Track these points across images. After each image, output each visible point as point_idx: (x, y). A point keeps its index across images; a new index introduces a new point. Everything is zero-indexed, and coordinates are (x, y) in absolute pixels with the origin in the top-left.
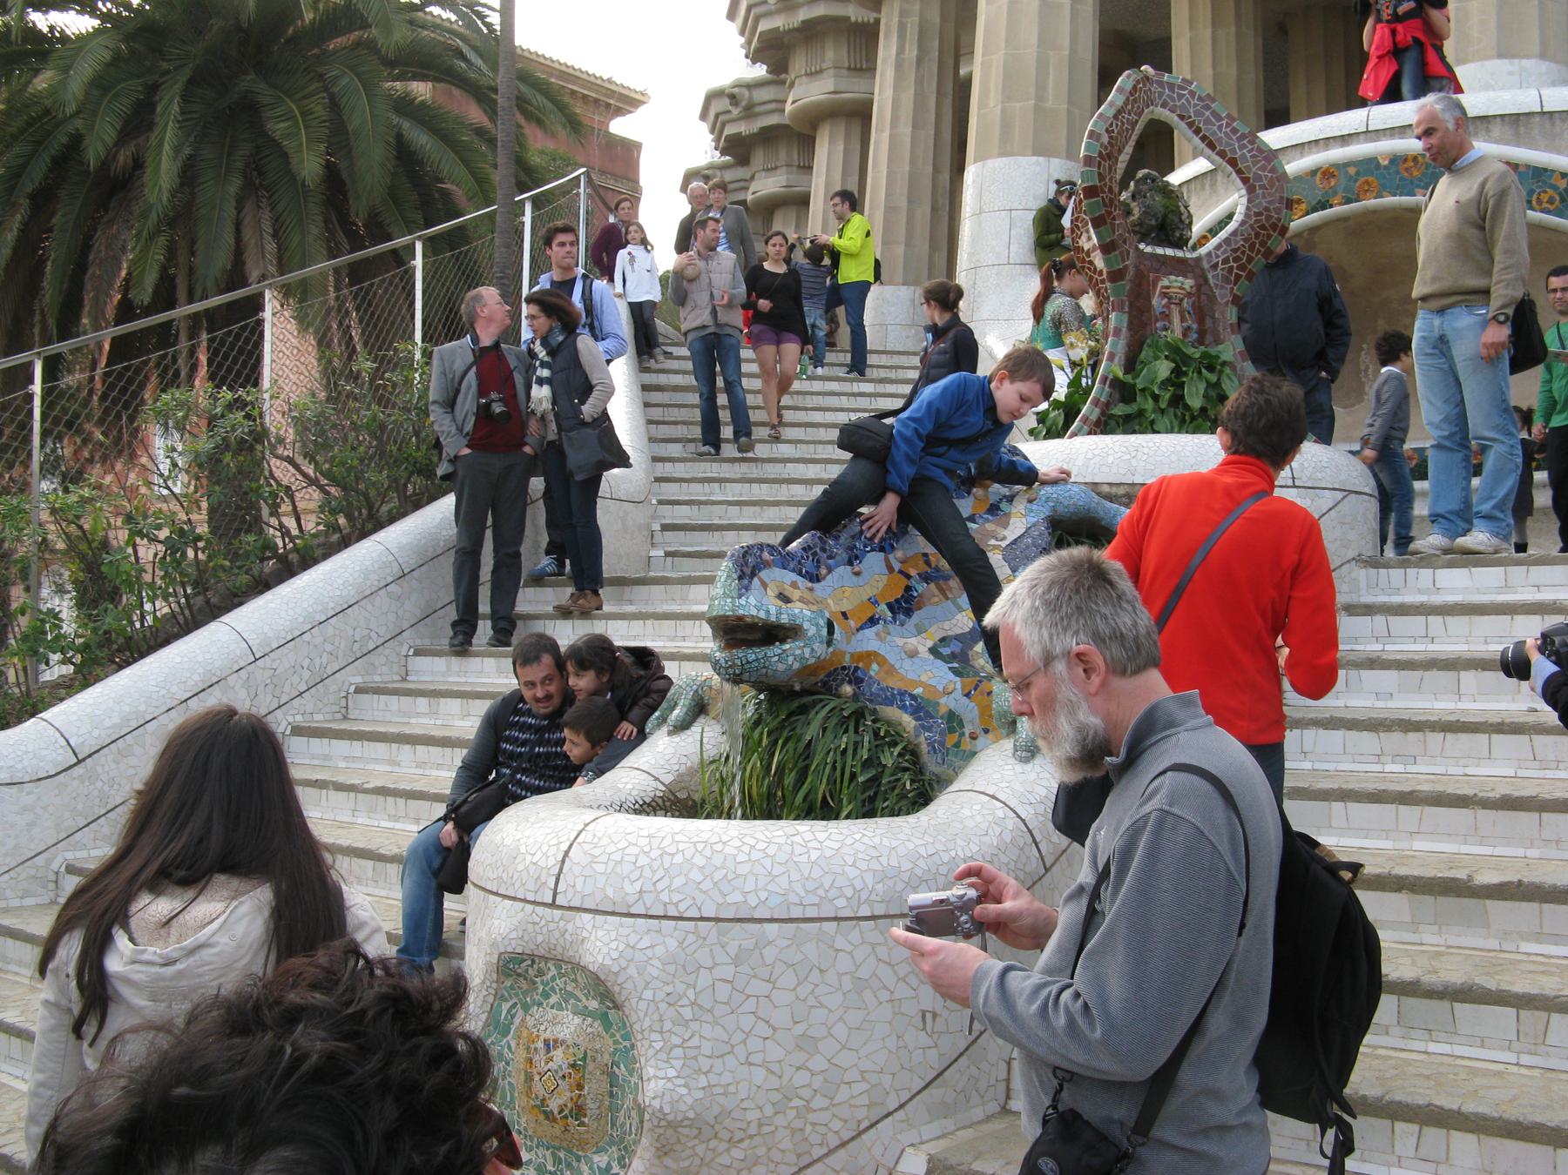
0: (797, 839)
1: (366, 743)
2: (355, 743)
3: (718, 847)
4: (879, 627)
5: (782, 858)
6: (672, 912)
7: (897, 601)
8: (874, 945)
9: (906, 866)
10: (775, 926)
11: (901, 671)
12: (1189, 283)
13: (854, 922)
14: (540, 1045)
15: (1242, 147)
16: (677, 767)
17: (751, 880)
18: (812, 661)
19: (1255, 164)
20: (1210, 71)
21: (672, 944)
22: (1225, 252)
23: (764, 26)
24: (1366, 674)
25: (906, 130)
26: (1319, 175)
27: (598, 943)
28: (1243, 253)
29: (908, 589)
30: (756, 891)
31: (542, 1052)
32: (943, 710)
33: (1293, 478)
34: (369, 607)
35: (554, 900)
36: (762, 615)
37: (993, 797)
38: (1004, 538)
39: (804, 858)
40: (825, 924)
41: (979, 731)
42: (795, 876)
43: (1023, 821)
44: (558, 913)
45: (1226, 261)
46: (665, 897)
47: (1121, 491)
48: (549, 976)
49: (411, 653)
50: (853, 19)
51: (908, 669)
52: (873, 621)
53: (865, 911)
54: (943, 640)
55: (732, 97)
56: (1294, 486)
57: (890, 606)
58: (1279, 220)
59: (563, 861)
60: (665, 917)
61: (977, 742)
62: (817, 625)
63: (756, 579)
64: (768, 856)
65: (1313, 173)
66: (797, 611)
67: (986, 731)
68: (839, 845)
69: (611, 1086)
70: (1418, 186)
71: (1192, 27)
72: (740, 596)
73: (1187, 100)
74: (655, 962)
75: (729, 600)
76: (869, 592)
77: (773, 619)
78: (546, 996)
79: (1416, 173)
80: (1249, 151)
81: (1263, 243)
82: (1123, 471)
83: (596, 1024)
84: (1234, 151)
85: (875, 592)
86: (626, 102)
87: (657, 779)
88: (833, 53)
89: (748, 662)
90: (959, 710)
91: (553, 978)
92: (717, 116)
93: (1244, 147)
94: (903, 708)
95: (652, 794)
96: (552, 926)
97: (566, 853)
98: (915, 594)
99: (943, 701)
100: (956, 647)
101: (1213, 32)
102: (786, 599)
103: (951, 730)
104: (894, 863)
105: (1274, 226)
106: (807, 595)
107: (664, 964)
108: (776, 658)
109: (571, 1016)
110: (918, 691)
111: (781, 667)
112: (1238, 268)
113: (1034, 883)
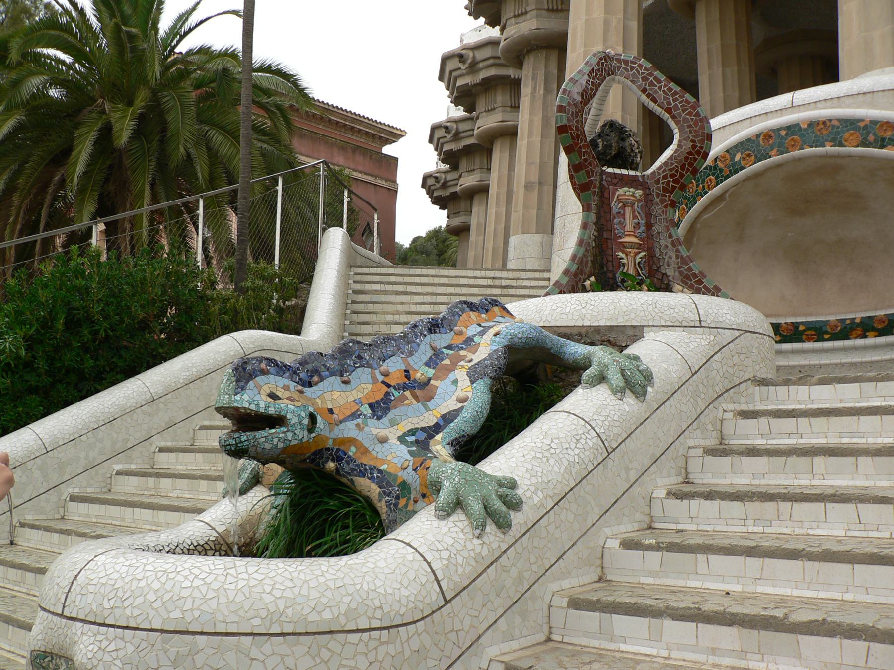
0: (233, 571)
1: (108, 506)
2: (102, 506)
3: (171, 576)
4: (359, 421)
5: (215, 585)
6: (132, 625)
7: (377, 402)
8: (282, 656)
9: (314, 594)
10: (204, 638)
11: (374, 453)
12: (639, 193)
13: (267, 637)
15: (675, 100)
16: (229, 521)
17: (190, 601)
18: (294, 442)
19: (684, 111)
20: (721, 95)
21: (130, 648)
23: (460, 83)
24: (746, 460)
25: (537, 139)
26: (762, 137)
28: (677, 171)
29: (387, 394)
30: (192, 610)
32: (399, 481)
33: (700, 321)
34: (129, 420)
35: (63, 612)
36: (253, 407)
37: (409, 545)
38: (470, 361)
39: (232, 586)
40: (243, 638)
41: (419, 496)
42: (223, 600)
43: (429, 564)
44: (64, 621)
45: (665, 177)
46: (128, 612)
47: (575, 331)
49: (157, 450)
50: (512, 77)
51: (378, 450)
52: (355, 415)
53: (276, 629)
54: (411, 430)
55: (446, 128)
56: (701, 327)
57: (371, 406)
58: (701, 148)
60: (127, 628)
62: (299, 416)
63: (251, 382)
64: (205, 583)
65: (758, 136)
66: (282, 406)
67: (424, 496)
68: (263, 577)
70: (827, 141)
71: (710, 68)
72: (236, 394)
73: (637, 70)
74: (118, 662)
75: (227, 396)
76: (355, 395)
77: (262, 410)
79: (825, 132)
80: (680, 103)
81: (691, 164)
82: (576, 317)
84: (669, 103)
85: (360, 395)
86: (393, 135)
87: (213, 528)
88: (501, 97)
89: (241, 442)
90: (409, 480)
92: (438, 139)
93: (676, 100)
94: (372, 479)
95: (206, 540)
98: (393, 398)
99: (400, 474)
100: (422, 436)
101: (723, 71)
102: (273, 396)
104: (304, 592)
105: (698, 153)
106: (296, 396)
107: (123, 664)
108: (263, 440)
110: (384, 467)
111: (268, 446)
112: (673, 182)
113: (433, 612)
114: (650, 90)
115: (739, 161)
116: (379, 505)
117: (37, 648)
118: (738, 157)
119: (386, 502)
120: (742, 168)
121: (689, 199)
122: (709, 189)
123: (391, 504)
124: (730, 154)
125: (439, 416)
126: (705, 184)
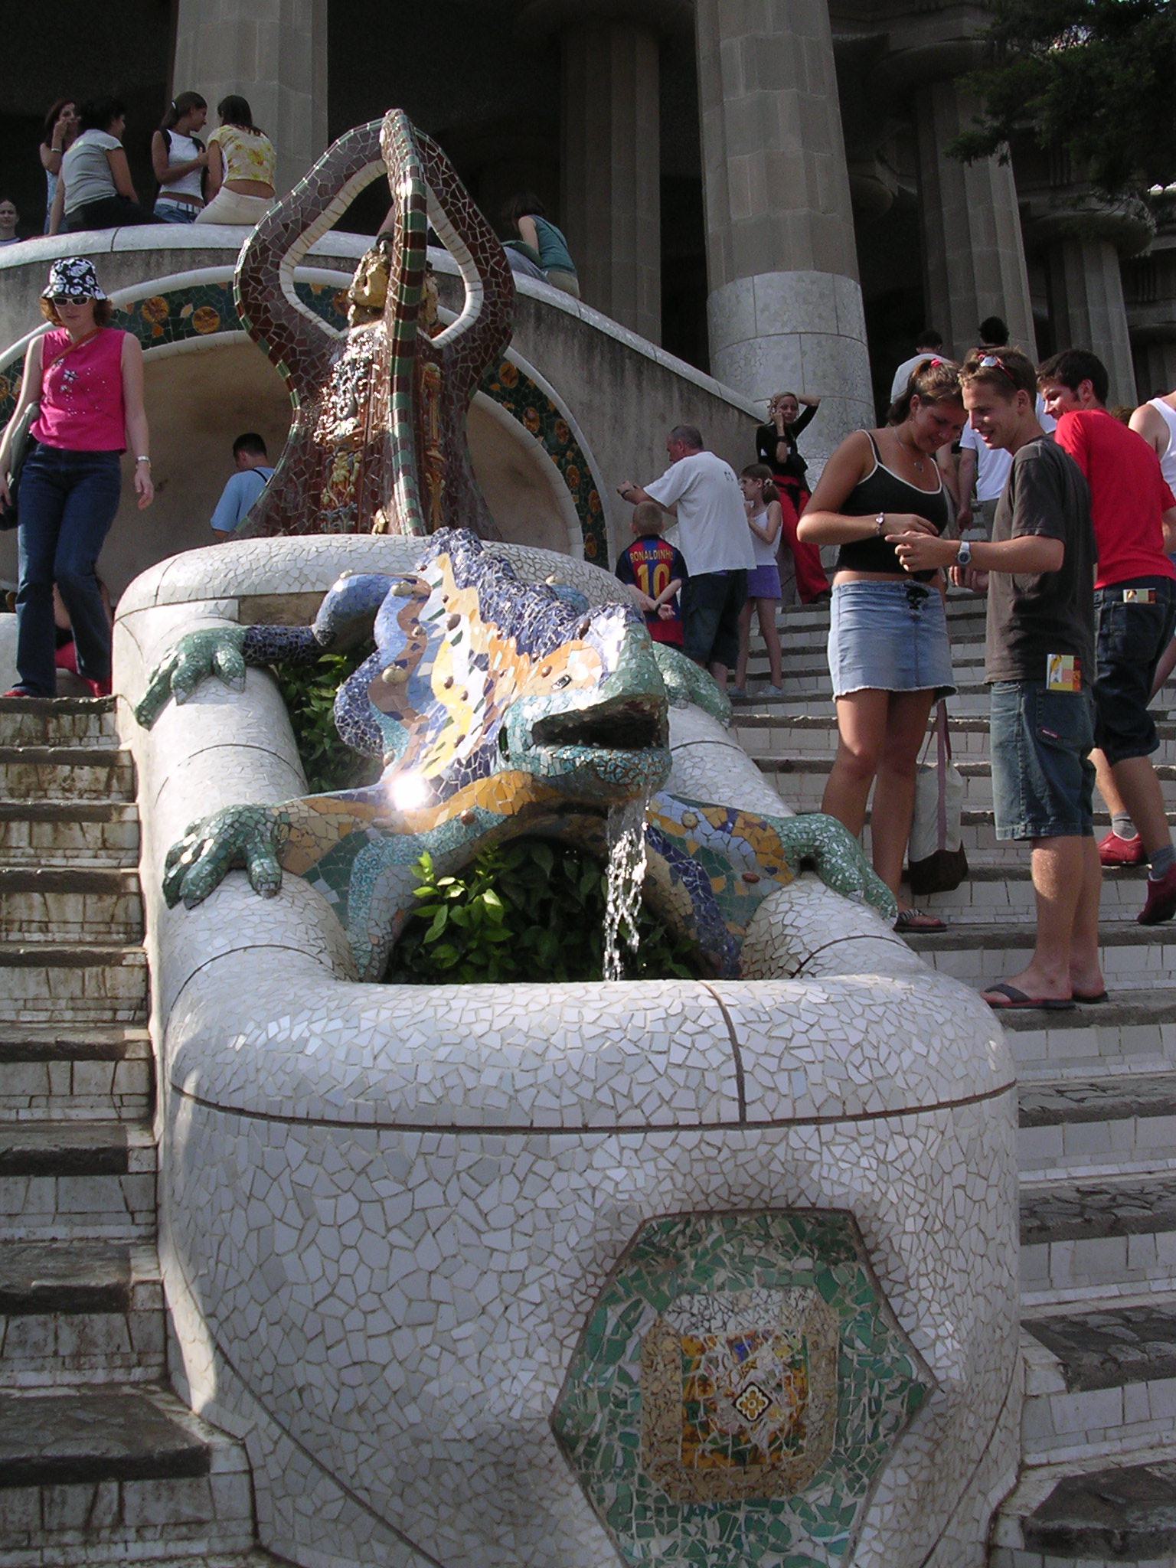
14: (720, 1350)
19: (493, 256)
22: (464, 349)
27: (841, 1164)
32: (692, 849)
44: (755, 1134)
45: (464, 360)
48: (708, 1243)
61: (760, 884)
67: (773, 871)
69: (841, 1378)
78: (705, 1273)
80: (489, 241)
83: (810, 1293)
84: (475, 238)
91: (718, 1242)
96: (742, 1157)
97: (733, 1038)
99: (688, 835)
103: (718, 874)
109: (764, 1293)
114: (453, 205)
115: (189, 319)
116: (673, 890)
117: (661, 1211)
118: (186, 312)
120: (193, 333)
123: (696, 888)
124: (171, 303)
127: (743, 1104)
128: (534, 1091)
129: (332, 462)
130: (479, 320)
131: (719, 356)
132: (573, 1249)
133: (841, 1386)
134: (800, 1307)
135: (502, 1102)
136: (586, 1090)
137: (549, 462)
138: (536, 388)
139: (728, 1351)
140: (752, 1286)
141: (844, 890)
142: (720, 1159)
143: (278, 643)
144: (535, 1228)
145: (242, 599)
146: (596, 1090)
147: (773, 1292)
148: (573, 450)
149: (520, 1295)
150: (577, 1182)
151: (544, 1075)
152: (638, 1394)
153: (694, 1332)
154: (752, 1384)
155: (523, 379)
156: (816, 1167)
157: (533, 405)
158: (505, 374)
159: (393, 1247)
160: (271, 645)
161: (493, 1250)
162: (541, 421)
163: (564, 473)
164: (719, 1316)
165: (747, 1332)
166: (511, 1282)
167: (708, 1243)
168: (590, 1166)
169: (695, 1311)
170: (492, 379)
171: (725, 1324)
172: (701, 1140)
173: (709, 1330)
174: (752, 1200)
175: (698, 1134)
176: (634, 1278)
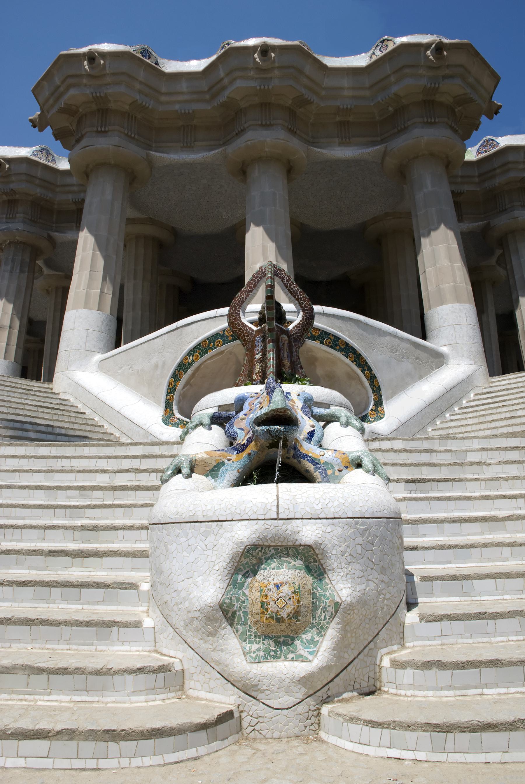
14: (272, 586)
19: (305, 302)
21: (340, 530)
28: (301, 331)
31: (275, 589)
45: (296, 333)
59: (278, 500)
67: (347, 467)
69: (313, 599)
74: (334, 538)
83: (302, 572)
93: (301, 295)
94: (308, 460)
97: (277, 496)
99: (321, 458)
109: (287, 571)
110: (310, 455)
119: (319, 472)
121: (202, 350)
122: (218, 346)
123: (323, 473)
125: (306, 434)
126: (215, 343)
127: (278, 513)
128: (219, 510)
129: (255, 367)
130: (301, 321)
131: (429, 334)
132: (227, 554)
133: (313, 602)
134: (298, 576)
135: (212, 514)
136: (233, 510)
137: (359, 371)
138: (352, 347)
139: (273, 587)
140: (283, 568)
141: (367, 472)
142: (271, 529)
143: (223, 416)
144: (218, 549)
145: (220, 406)
146: (236, 509)
147: (290, 571)
148: (367, 366)
149: (214, 568)
150: (229, 535)
151: (222, 506)
152: (248, 599)
153: (264, 581)
154: (281, 597)
155: (347, 344)
156: (301, 532)
157: (351, 352)
158: (341, 343)
159: (184, 556)
160: (221, 417)
161: (208, 556)
162: (355, 358)
163: (364, 374)
164: (272, 577)
165: (280, 582)
166: (212, 564)
167: (270, 555)
168: (233, 531)
169: (265, 575)
170: (336, 345)
171: (273, 579)
172: (265, 524)
173: (268, 581)
174: (282, 542)
175: (264, 521)
176: (246, 564)
